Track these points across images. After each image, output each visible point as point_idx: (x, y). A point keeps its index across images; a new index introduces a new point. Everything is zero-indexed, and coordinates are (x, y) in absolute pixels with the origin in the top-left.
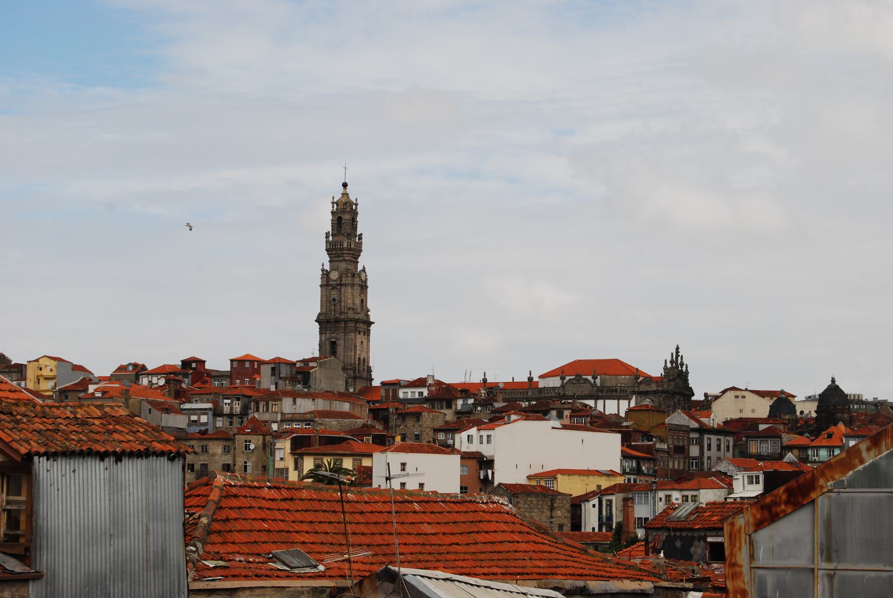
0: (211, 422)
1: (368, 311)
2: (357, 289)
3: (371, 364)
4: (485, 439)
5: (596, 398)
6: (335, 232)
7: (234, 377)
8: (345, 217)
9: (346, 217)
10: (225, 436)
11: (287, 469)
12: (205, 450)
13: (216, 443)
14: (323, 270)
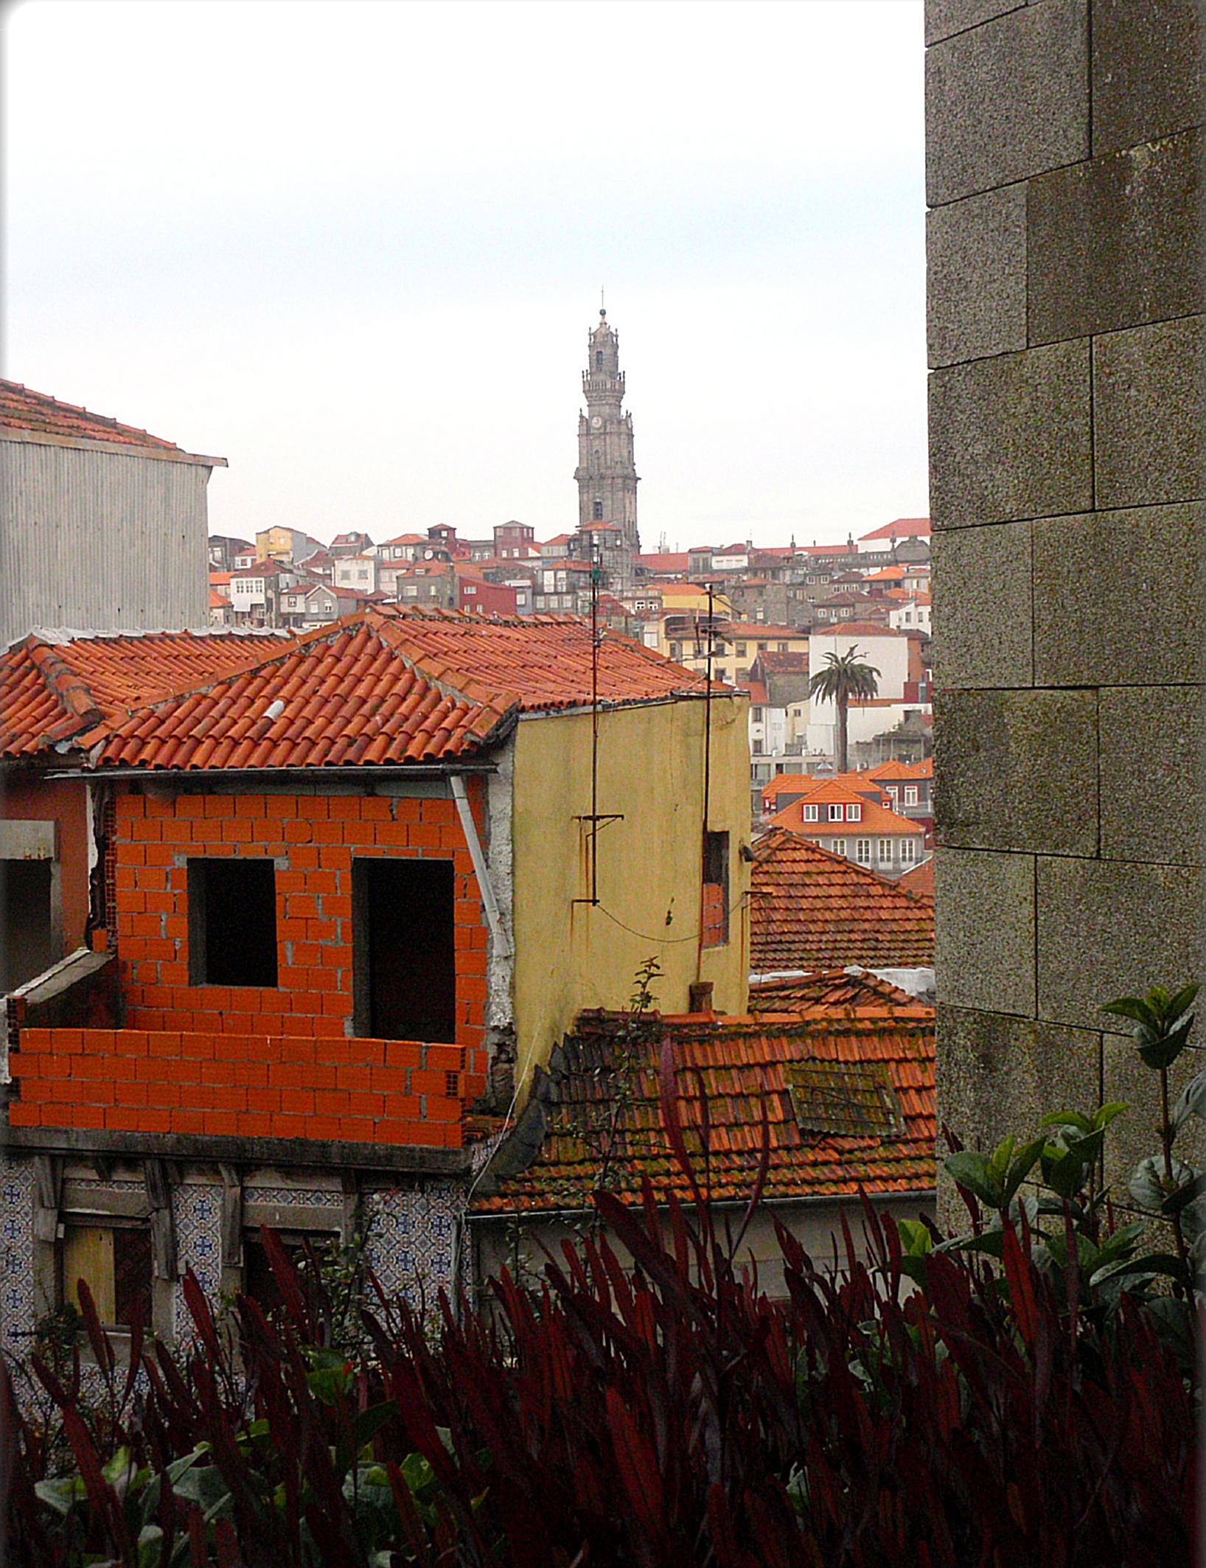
7: (500, 546)
8: (604, 351)
9: (607, 351)
14: (581, 417)
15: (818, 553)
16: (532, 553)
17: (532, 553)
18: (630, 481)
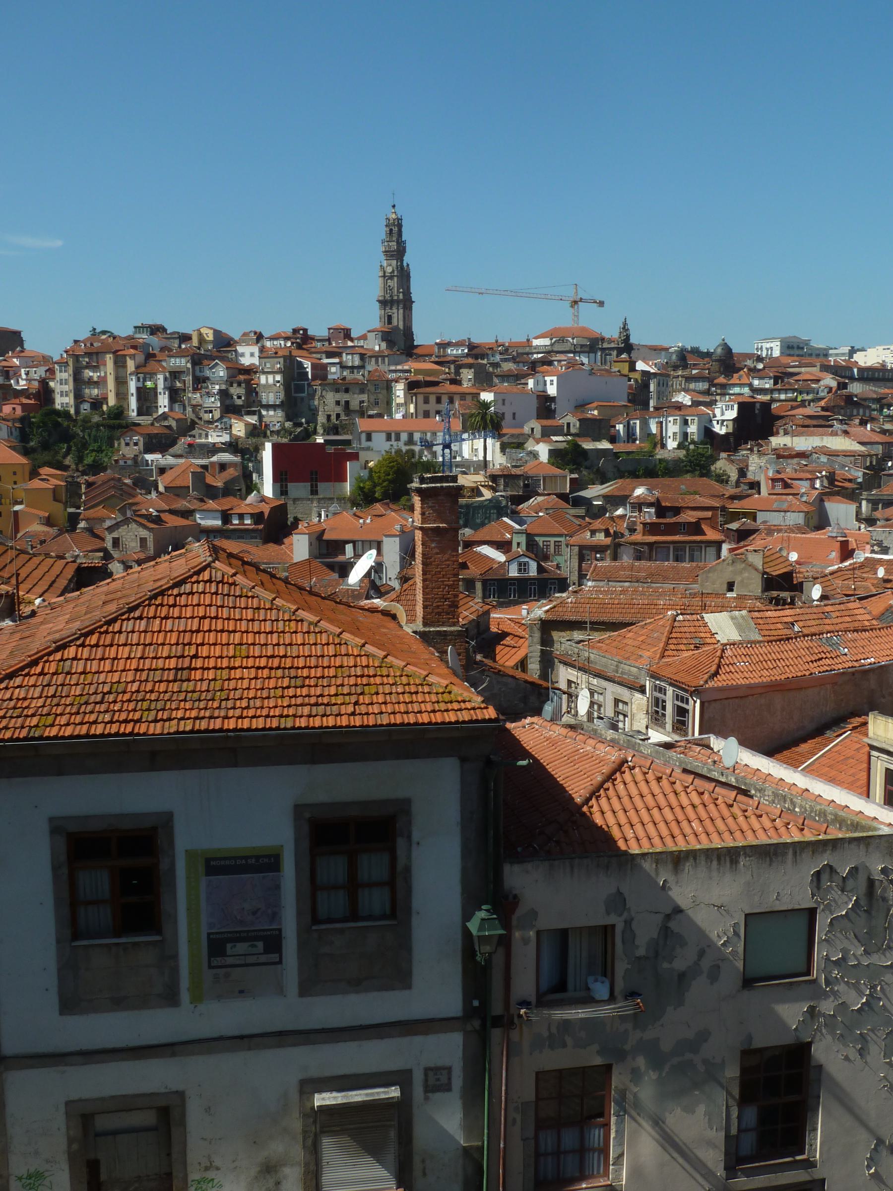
5: (574, 352)
8: (395, 229)
16: (350, 344)
17: (350, 344)
18: (407, 303)
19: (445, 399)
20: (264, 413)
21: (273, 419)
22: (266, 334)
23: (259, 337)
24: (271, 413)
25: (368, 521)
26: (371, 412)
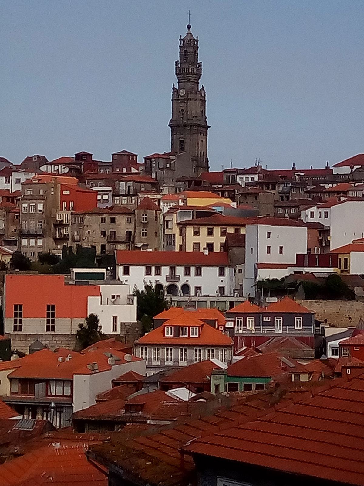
0: (110, 200)
1: (206, 118)
2: (199, 102)
3: (208, 157)
4: (323, 215)
6: (182, 61)
8: (189, 51)
9: (190, 50)
10: (127, 211)
11: (174, 235)
12: (113, 221)
13: (121, 216)
14: (174, 89)
15: (310, 173)
16: (134, 170)
17: (134, 170)
19: (217, 231)
20: (24, 242)
21: (33, 250)
22: (50, 161)
23: (42, 161)
24: (32, 242)
25: (67, 359)
26: (139, 245)
